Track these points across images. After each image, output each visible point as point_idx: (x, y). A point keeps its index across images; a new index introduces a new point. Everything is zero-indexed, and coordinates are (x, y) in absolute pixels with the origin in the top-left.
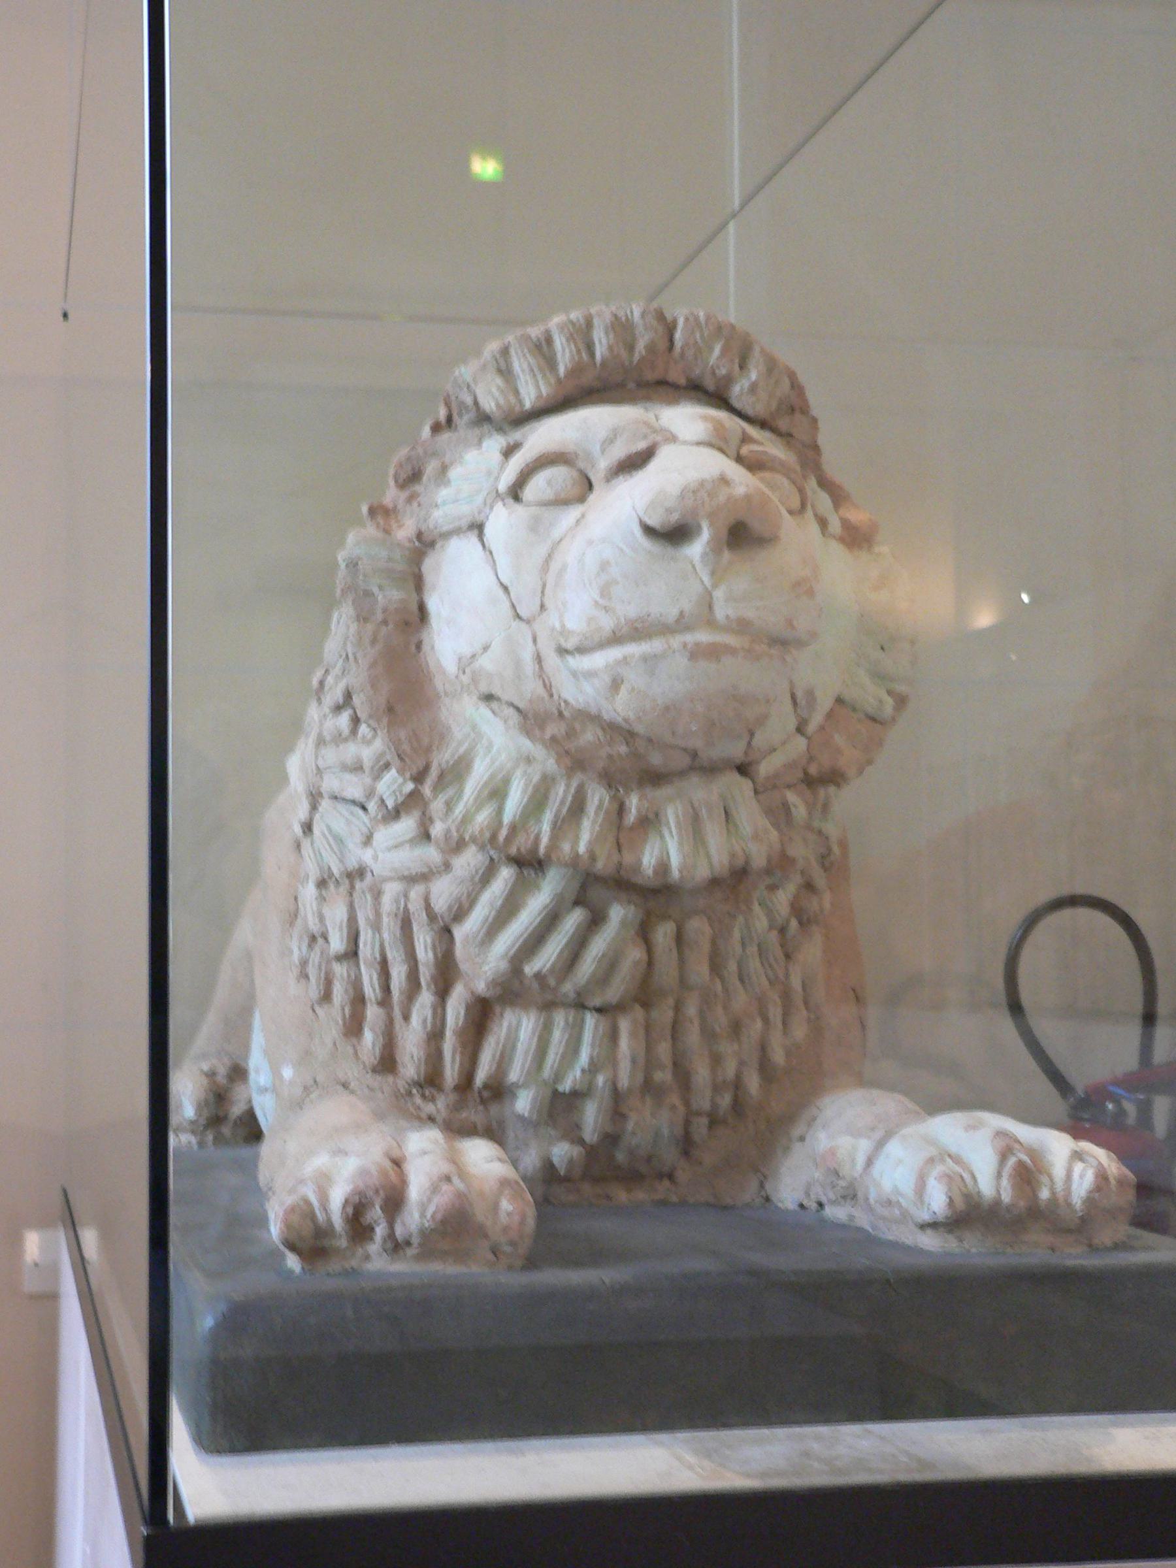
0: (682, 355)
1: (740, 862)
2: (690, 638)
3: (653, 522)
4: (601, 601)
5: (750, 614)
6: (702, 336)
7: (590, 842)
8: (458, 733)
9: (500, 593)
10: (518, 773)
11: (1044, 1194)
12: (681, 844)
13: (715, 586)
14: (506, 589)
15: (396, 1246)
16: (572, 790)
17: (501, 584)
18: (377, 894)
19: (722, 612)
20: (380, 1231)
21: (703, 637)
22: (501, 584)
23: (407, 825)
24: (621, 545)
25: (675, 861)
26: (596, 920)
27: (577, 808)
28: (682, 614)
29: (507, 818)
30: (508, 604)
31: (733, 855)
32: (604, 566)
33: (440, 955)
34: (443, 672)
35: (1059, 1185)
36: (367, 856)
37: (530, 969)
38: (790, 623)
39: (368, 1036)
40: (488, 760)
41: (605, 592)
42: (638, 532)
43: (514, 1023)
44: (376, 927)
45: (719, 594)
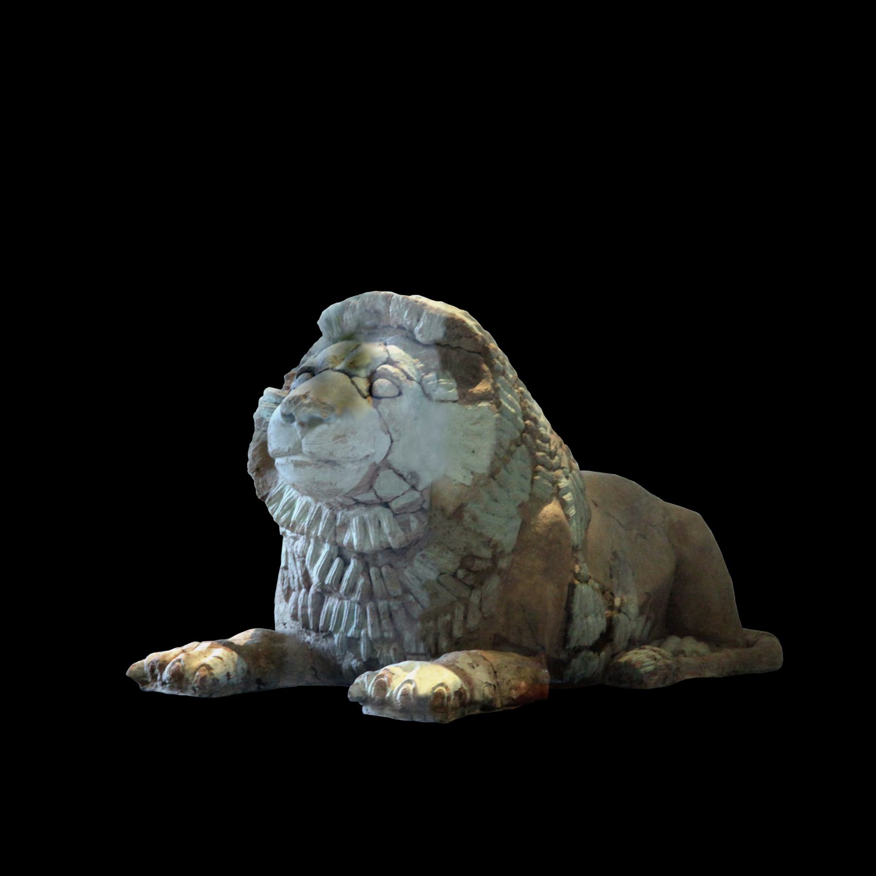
0: (393, 316)
1: (385, 546)
2: (294, 458)
5: (314, 451)
6: (399, 307)
7: (321, 531)
11: (388, 695)
12: (357, 536)
13: (302, 437)
15: (164, 684)
16: (317, 509)
19: (305, 449)
20: (159, 677)
21: (298, 458)
25: (355, 542)
26: (346, 564)
27: (318, 516)
28: (289, 450)
31: (381, 542)
33: (303, 571)
35: (394, 692)
37: (327, 581)
38: (331, 454)
39: (290, 604)
40: (288, 494)
43: (331, 604)
45: (303, 441)
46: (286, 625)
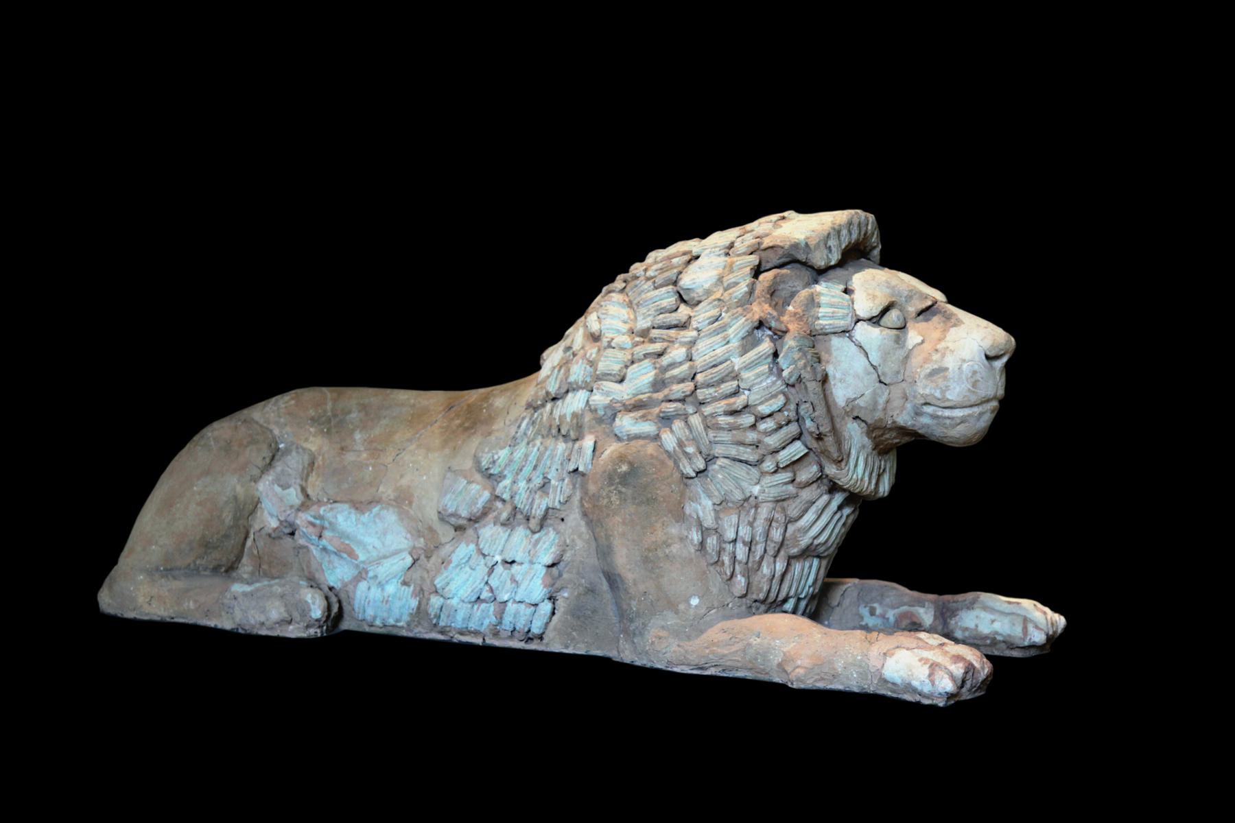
3: (988, 353)
4: (971, 388)
8: (846, 434)
9: (873, 371)
10: (861, 454)
14: (875, 368)
17: (872, 365)
18: (756, 507)
22: (872, 365)
23: (785, 476)
24: (979, 363)
29: (860, 477)
30: (877, 375)
32: (975, 373)
34: (836, 404)
36: (756, 490)
41: (975, 384)
42: (984, 358)
44: (751, 524)
46: (730, 606)
